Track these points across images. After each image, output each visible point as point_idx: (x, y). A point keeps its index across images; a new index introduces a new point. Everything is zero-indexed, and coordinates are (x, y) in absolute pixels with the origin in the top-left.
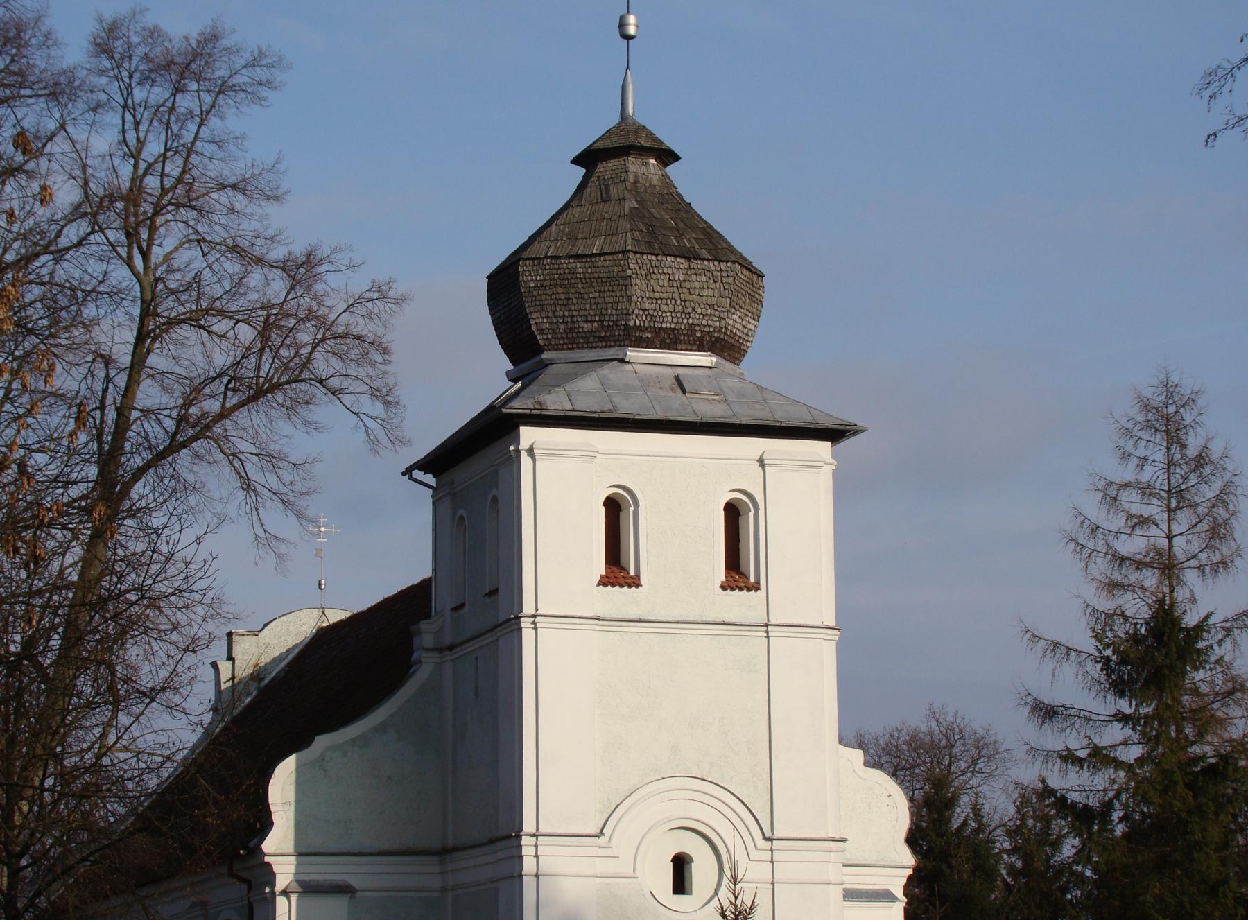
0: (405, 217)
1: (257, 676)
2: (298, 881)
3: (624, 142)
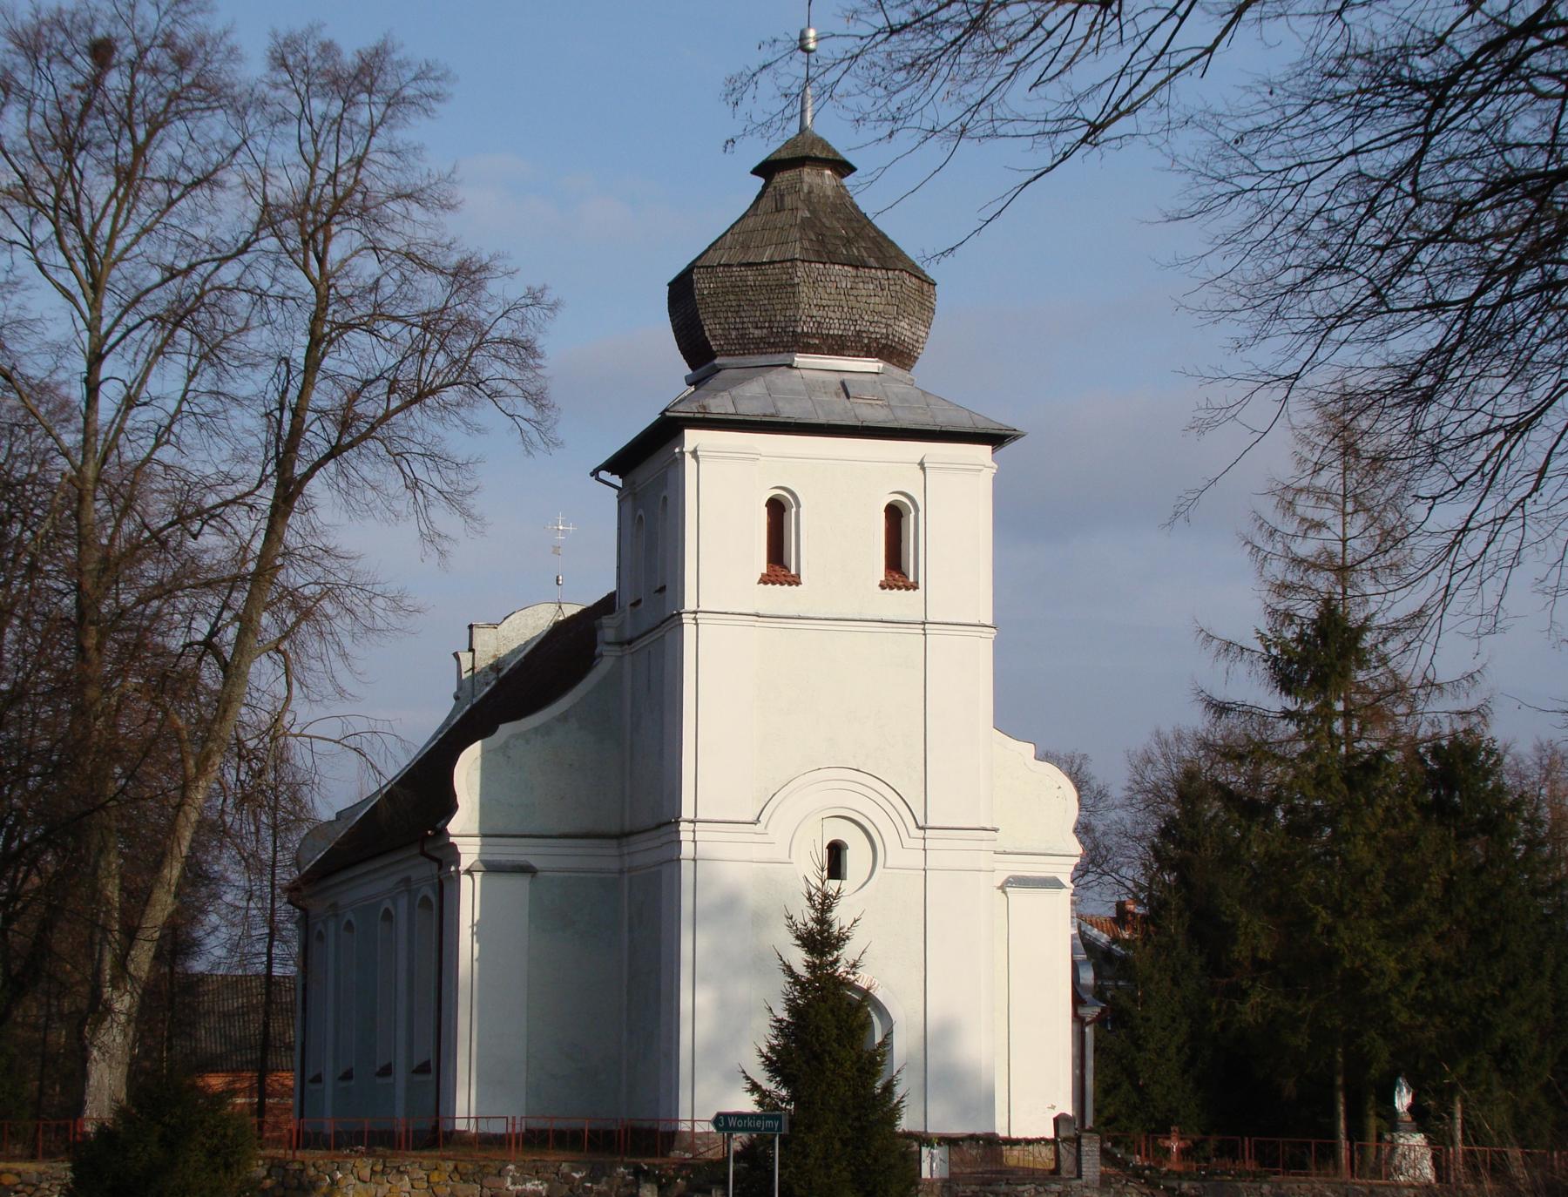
0: (580, 227)
1: (495, 667)
2: (482, 861)
3: (799, 153)
